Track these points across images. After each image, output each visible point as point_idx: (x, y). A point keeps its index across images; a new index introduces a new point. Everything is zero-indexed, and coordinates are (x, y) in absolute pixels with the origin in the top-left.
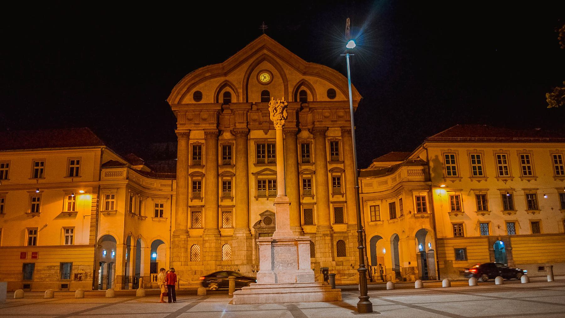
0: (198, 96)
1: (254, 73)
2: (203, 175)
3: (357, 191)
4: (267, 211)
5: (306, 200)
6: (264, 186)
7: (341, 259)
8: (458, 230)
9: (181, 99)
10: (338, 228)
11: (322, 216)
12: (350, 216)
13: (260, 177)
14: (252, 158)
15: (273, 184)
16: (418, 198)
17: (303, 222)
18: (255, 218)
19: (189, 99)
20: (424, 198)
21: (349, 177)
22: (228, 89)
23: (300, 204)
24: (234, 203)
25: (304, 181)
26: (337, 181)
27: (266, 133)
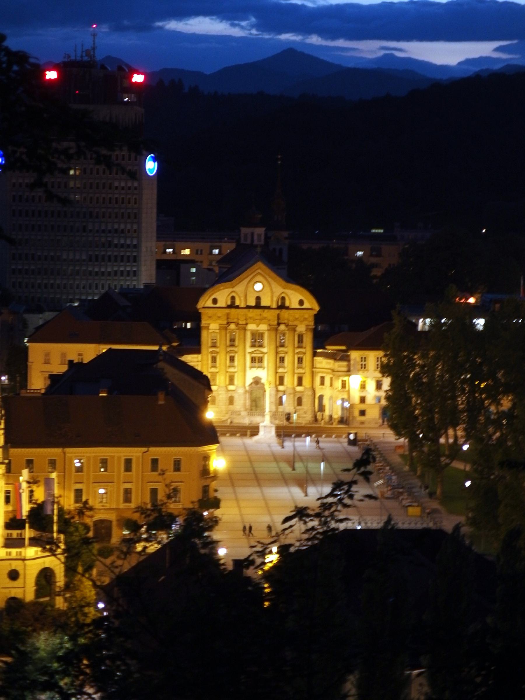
0: (215, 301)
1: (252, 283)
2: (217, 353)
3: (313, 366)
4: (257, 377)
5: (280, 370)
6: (255, 360)
7: (299, 407)
8: (363, 400)
9: (205, 303)
10: (299, 389)
11: (289, 381)
12: (306, 381)
13: (253, 355)
14: (248, 343)
15: (261, 360)
16: (343, 381)
17: (278, 383)
18: (249, 380)
19: (209, 303)
20: (345, 381)
21: (307, 358)
22: (233, 294)
23: (277, 373)
24: (235, 370)
25: (280, 358)
26: (300, 360)
27: (258, 326)
